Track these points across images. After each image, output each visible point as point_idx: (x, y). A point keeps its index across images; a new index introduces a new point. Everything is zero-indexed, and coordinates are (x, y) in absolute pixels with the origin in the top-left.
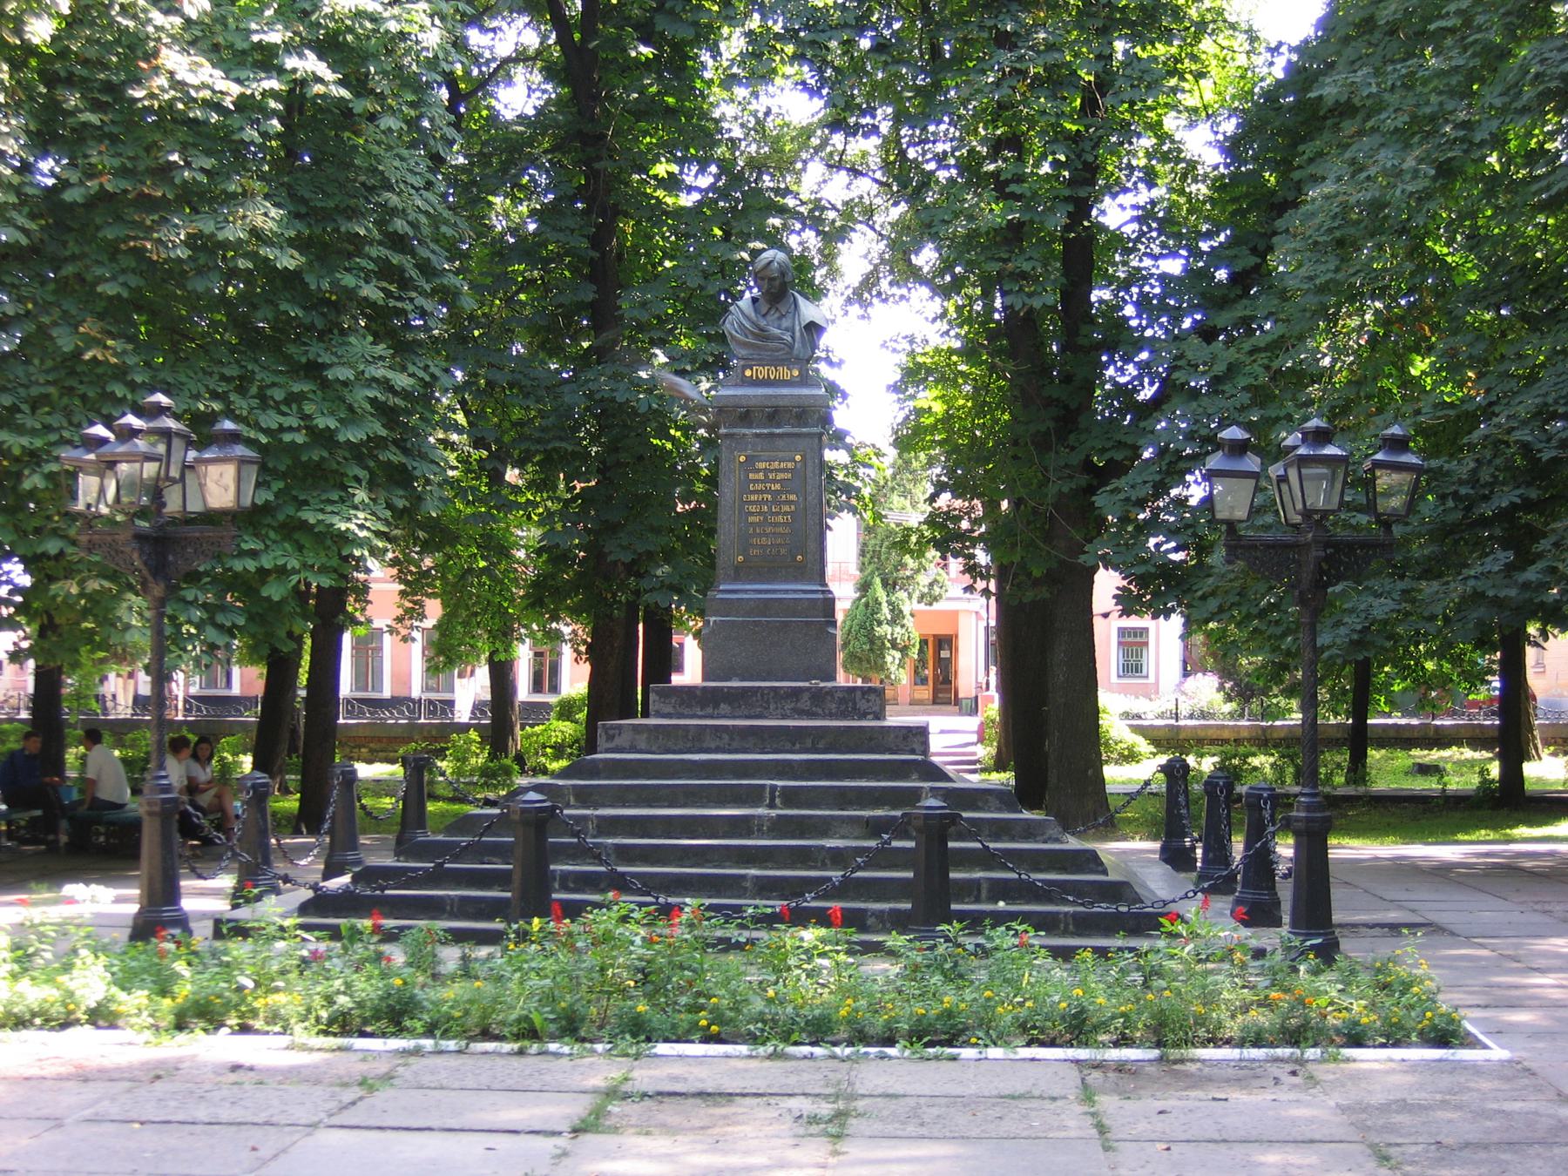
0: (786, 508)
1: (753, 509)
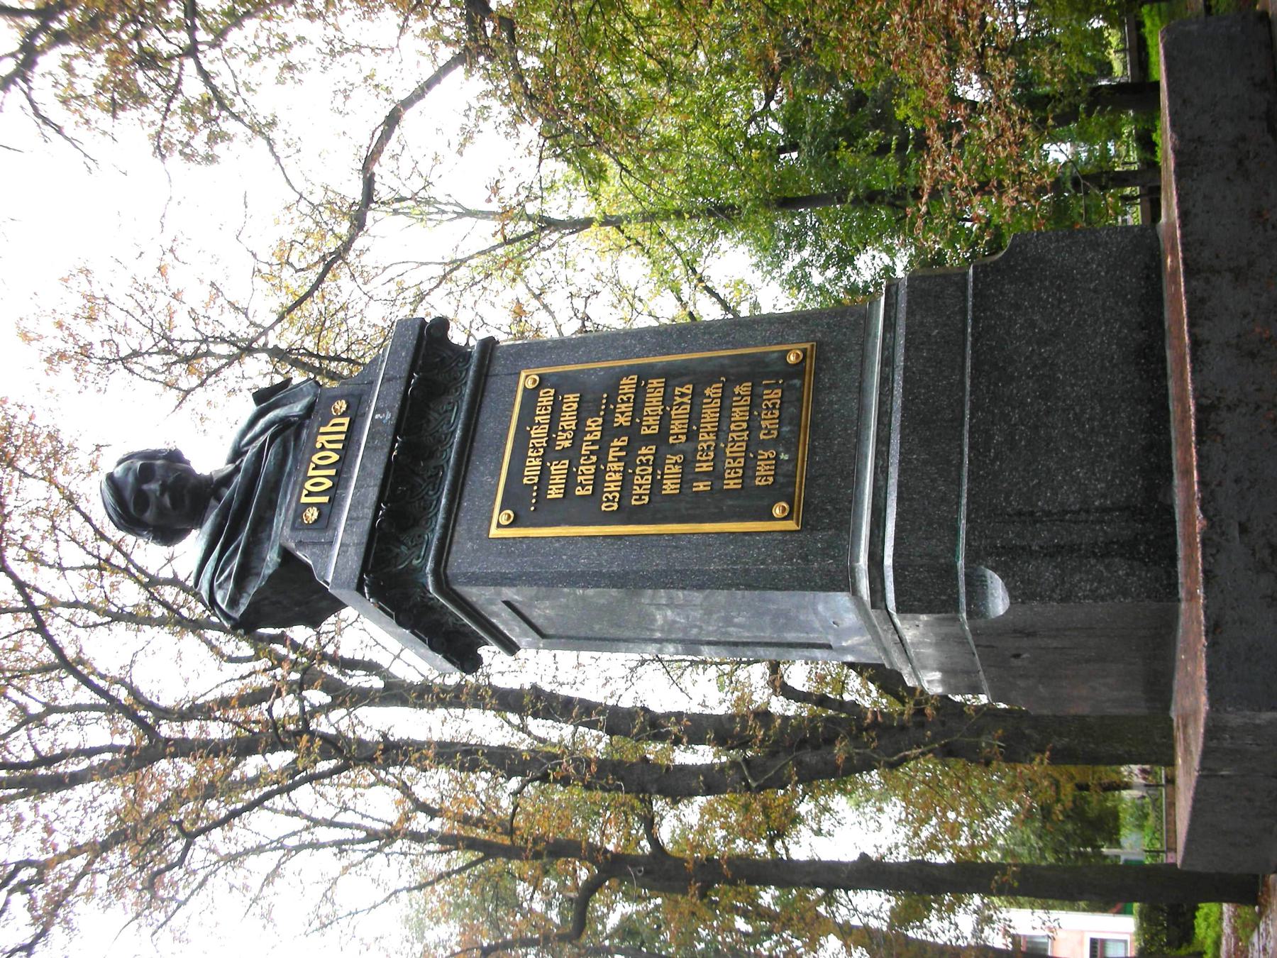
0: (654, 400)
1: (642, 484)
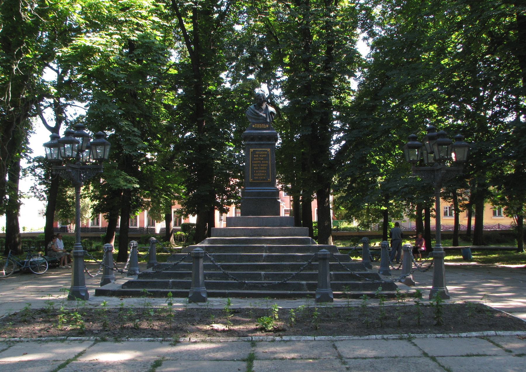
0: (265, 165)
1: (255, 165)
